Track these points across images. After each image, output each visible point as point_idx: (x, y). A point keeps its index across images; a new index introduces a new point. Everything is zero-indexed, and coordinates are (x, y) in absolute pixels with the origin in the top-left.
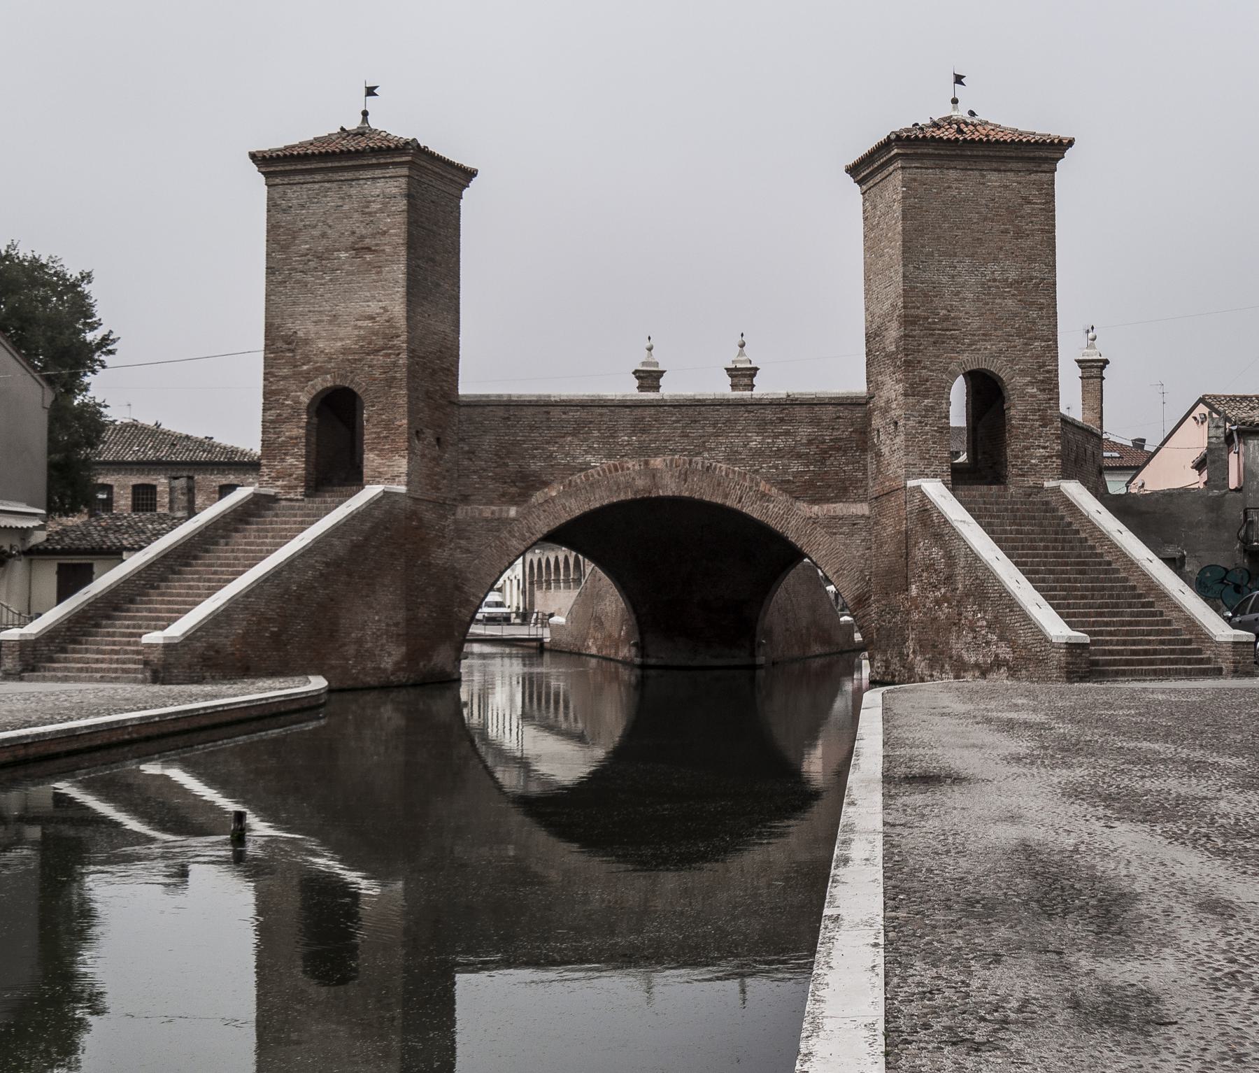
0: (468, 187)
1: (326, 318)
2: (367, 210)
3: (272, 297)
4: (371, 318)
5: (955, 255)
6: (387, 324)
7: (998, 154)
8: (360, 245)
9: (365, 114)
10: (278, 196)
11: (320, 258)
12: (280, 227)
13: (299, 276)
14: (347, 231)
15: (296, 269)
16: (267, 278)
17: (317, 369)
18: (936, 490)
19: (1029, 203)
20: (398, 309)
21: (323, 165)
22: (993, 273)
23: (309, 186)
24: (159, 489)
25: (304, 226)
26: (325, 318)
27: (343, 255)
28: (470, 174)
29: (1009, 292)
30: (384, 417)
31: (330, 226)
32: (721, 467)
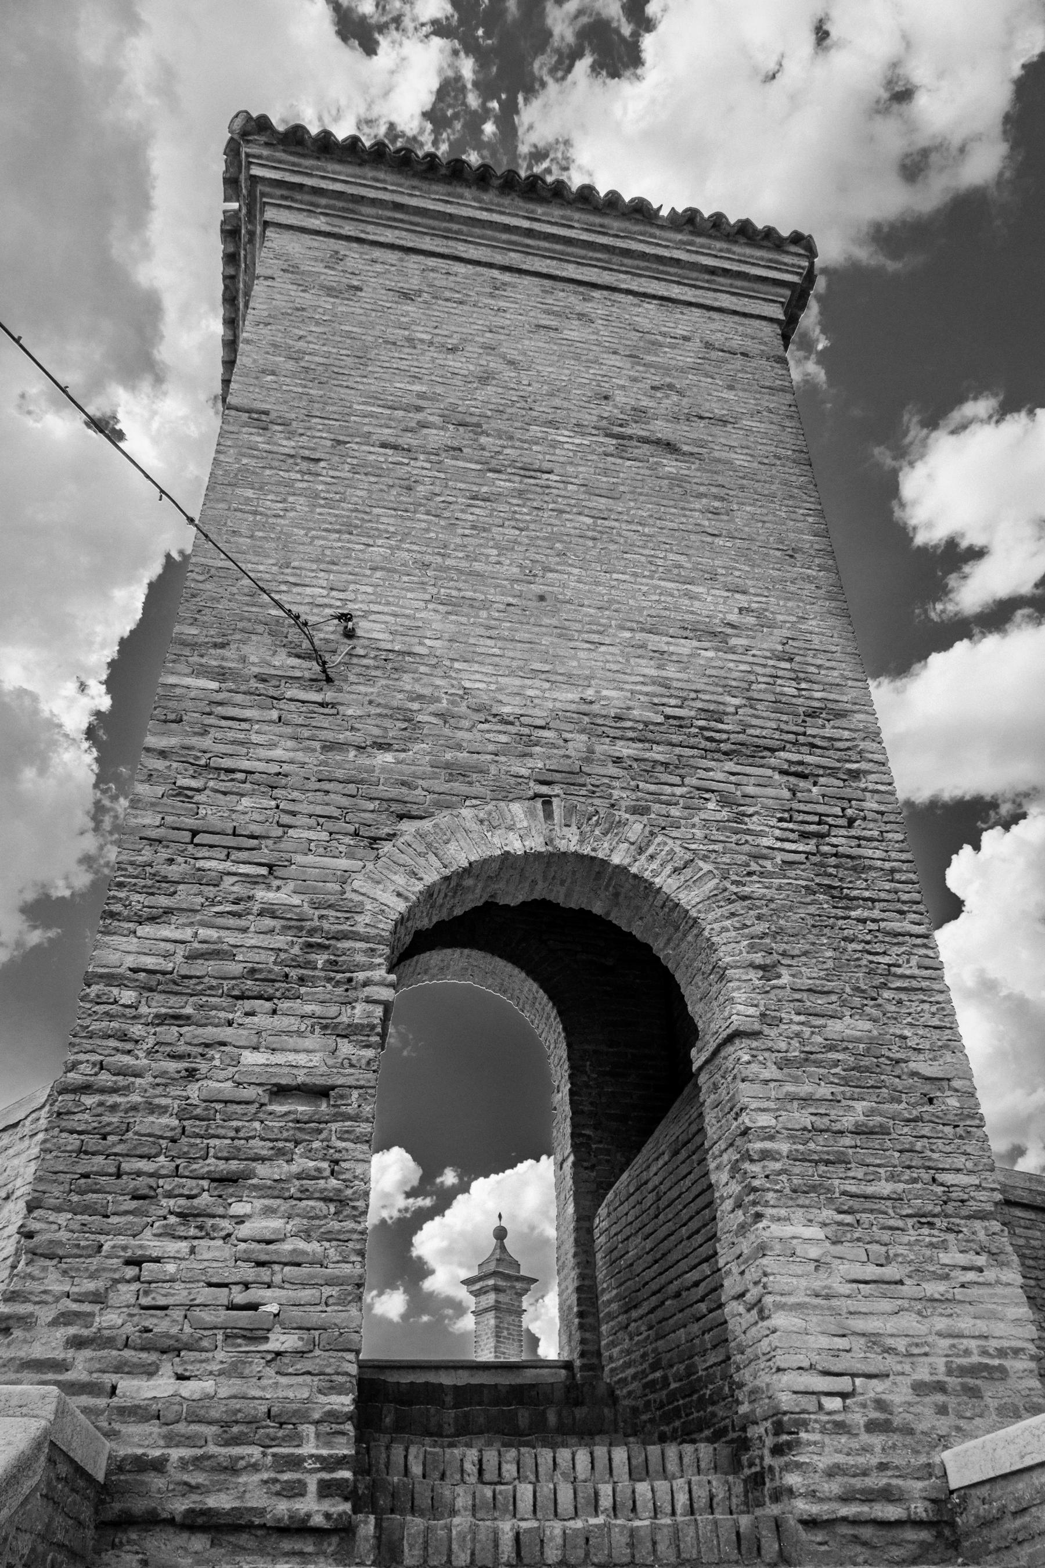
2: (649, 358)
6: (786, 665)
17: (457, 772)
23: (431, 262)
30: (835, 1028)
31: (511, 363)
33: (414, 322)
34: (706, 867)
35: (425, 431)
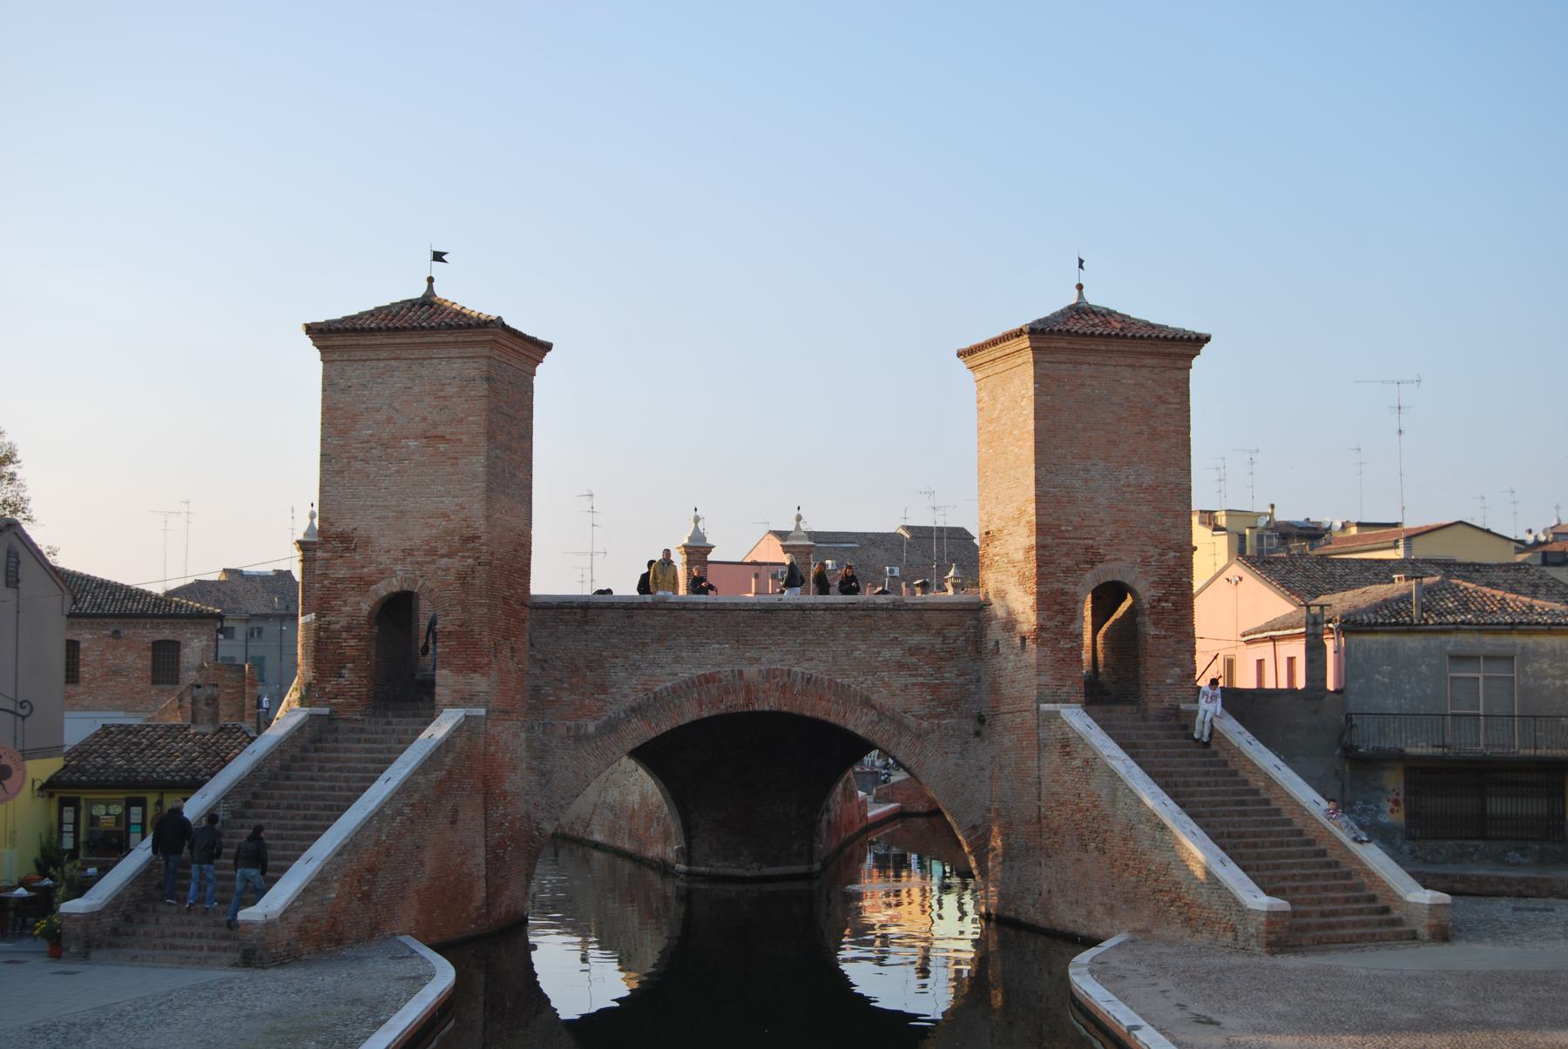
0: (542, 362)
1: (391, 514)
3: (327, 489)
4: (445, 516)
5: (1089, 457)
6: (464, 522)
7: (1134, 349)
8: (433, 432)
9: (431, 280)
10: (336, 373)
11: (385, 446)
12: (337, 409)
13: (359, 465)
14: (417, 416)
15: (356, 457)
16: (321, 466)
18: (1076, 718)
19: (1164, 402)
20: (477, 507)
21: (391, 341)
22: (1127, 477)
23: (373, 363)
24: (82, 646)
25: (367, 408)
26: (391, 514)
27: (413, 444)
28: (547, 347)
29: (1144, 498)
31: (397, 410)
32: (822, 679)
33: (368, 399)
34: (436, 590)
35: (373, 451)
